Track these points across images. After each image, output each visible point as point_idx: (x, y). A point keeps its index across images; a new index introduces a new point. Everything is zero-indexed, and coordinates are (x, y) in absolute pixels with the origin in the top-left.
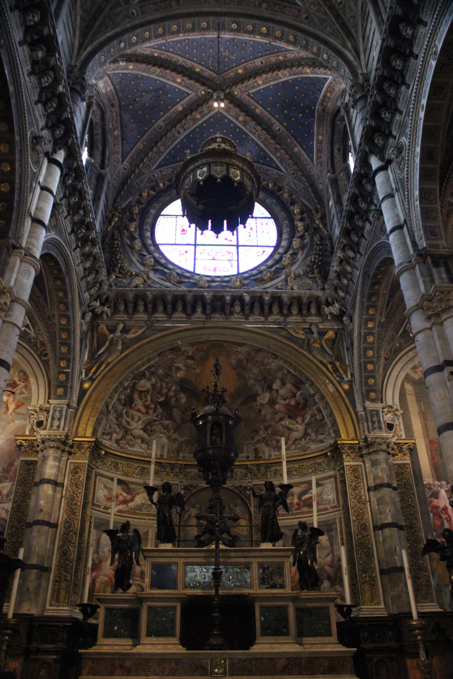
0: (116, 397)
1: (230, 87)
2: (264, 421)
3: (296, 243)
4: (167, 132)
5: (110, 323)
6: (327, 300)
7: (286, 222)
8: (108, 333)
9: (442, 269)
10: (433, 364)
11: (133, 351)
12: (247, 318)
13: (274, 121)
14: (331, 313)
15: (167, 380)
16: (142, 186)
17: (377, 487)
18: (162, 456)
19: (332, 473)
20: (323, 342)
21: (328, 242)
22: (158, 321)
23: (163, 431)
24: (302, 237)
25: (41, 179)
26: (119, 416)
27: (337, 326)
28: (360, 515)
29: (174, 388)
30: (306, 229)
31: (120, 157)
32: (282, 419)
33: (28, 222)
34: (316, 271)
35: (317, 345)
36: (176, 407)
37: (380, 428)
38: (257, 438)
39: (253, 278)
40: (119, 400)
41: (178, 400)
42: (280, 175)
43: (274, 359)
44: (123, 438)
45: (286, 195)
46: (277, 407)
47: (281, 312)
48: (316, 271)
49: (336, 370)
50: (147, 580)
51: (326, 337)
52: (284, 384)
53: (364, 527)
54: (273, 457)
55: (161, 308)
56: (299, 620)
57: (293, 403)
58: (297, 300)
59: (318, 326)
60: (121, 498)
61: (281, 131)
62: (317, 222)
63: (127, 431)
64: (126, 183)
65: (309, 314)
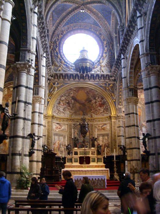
0: (56, 102)
1: (86, 5)
2: (93, 107)
3: (104, 55)
4: (66, 17)
5: (53, 82)
6: (111, 75)
7: (102, 47)
8: (53, 85)
9: (131, 92)
10: (126, 113)
11: (60, 90)
13: (99, 13)
14: (112, 79)
15: (69, 97)
16: (59, 33)
17: (119, 127)
18: (68, 116)
19: (109, 122)
20: (109, 87)
21: (113, 55)
22: (66, 81)
23: (68, 110)
24: (106, 53)
25: (42, 64)
26: (57, 107)
28: (115, 133)
29: (70, 99)
30: (107, 50)
31: (52, 26)
32: (98, 107)
33: (42, 77)
35: (108, 88)
36: (71, 103)
37: (121, 112)
38: (92, 112)
40: (57, 103)
41: (71, 102)
42: (100, 29)
44: (58, 112)
45: (102, 37)
46: (97, 104)
47: (99, 79)
48: (109, 65)
49: (112, 96)
50: (73, 154)
51: (110, 86)
52: (99, 98)
53: (115, 136)
54: (95, 117)
55: (67, 78)
56: (97, 160)
57: (101, 103)
59: (108, 83)
60: (59, 128)
63: (59, 111)
64: (54, 33)
65: (106, 79)
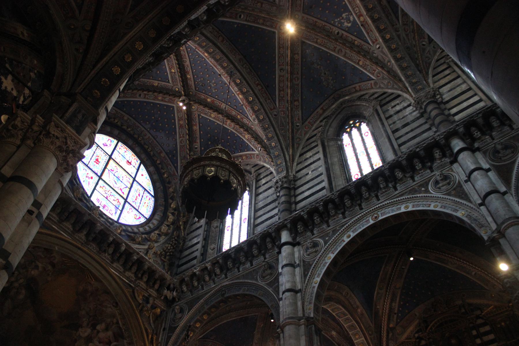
6: (170, 285)
12: (112, 263)
14: (166, 297)
20: (151, 314)
27: (164, 307)
30: (173, 223)
34: (167, 257)
39: (128, 233)
43: (113, 306)
45: (171, 190)
47: (135, 274)
52: (107, 329)
58: (151, 272)
61: (197, 150)
62: (181, 223)
65: (152, 287)
